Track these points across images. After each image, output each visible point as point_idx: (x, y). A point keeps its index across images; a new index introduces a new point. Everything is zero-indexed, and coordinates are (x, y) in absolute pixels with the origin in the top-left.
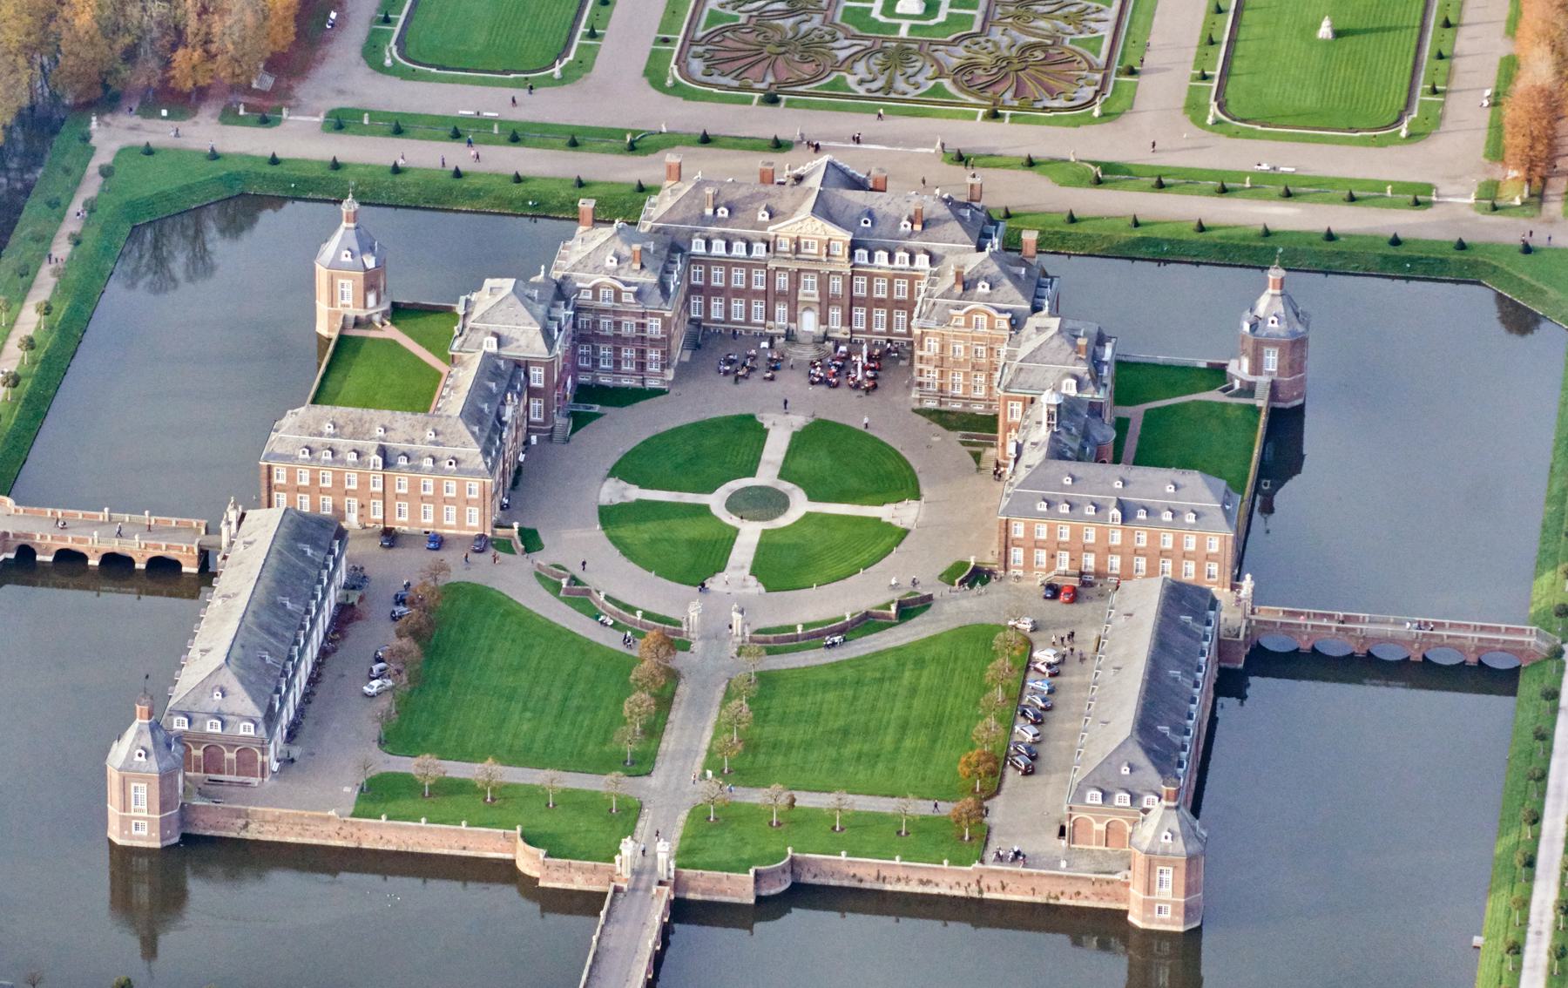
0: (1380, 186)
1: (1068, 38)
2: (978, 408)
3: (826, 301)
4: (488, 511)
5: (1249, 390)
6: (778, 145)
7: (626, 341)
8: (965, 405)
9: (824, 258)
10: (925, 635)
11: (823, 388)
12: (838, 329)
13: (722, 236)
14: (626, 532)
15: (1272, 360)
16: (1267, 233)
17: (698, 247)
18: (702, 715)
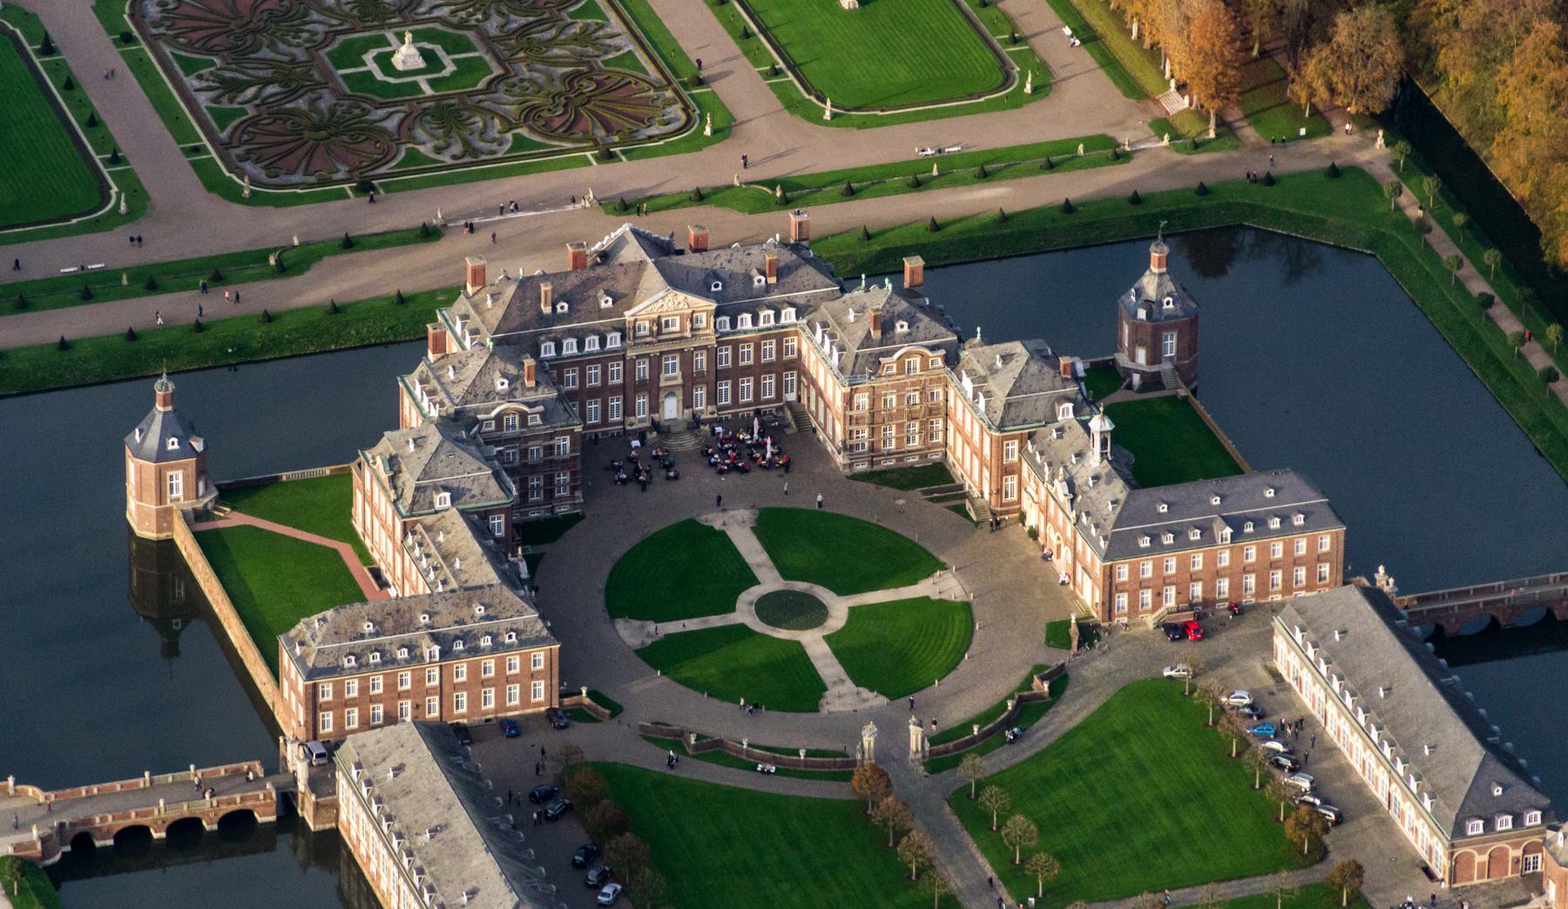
0: (1068, 146)
1: (599, 61)
2: (913, 460)
3: (691, 380)
4: (556, 681)
5: (1153, 381)
6: (429, 234)
7: (533, 469)
8: (899, 460)
9: (688, 334)
10: (1094, 707)
11: (734, 476)
12: (702, 407)
13: (570, 333)
14: (688, 671)
15: (1171, 344)
16: (1004, 219)
17: (548, 351)
18: (961, 847)
